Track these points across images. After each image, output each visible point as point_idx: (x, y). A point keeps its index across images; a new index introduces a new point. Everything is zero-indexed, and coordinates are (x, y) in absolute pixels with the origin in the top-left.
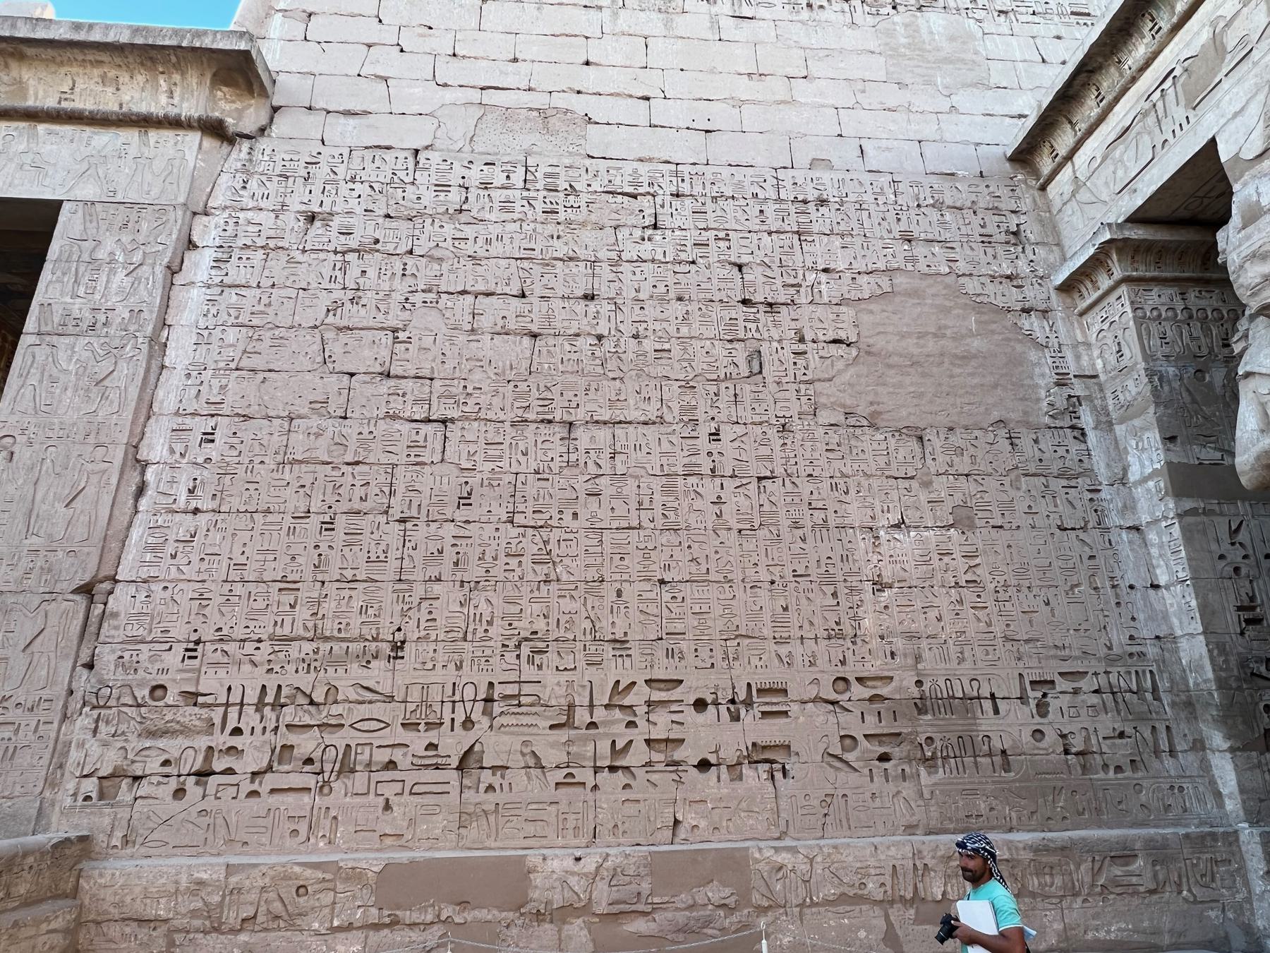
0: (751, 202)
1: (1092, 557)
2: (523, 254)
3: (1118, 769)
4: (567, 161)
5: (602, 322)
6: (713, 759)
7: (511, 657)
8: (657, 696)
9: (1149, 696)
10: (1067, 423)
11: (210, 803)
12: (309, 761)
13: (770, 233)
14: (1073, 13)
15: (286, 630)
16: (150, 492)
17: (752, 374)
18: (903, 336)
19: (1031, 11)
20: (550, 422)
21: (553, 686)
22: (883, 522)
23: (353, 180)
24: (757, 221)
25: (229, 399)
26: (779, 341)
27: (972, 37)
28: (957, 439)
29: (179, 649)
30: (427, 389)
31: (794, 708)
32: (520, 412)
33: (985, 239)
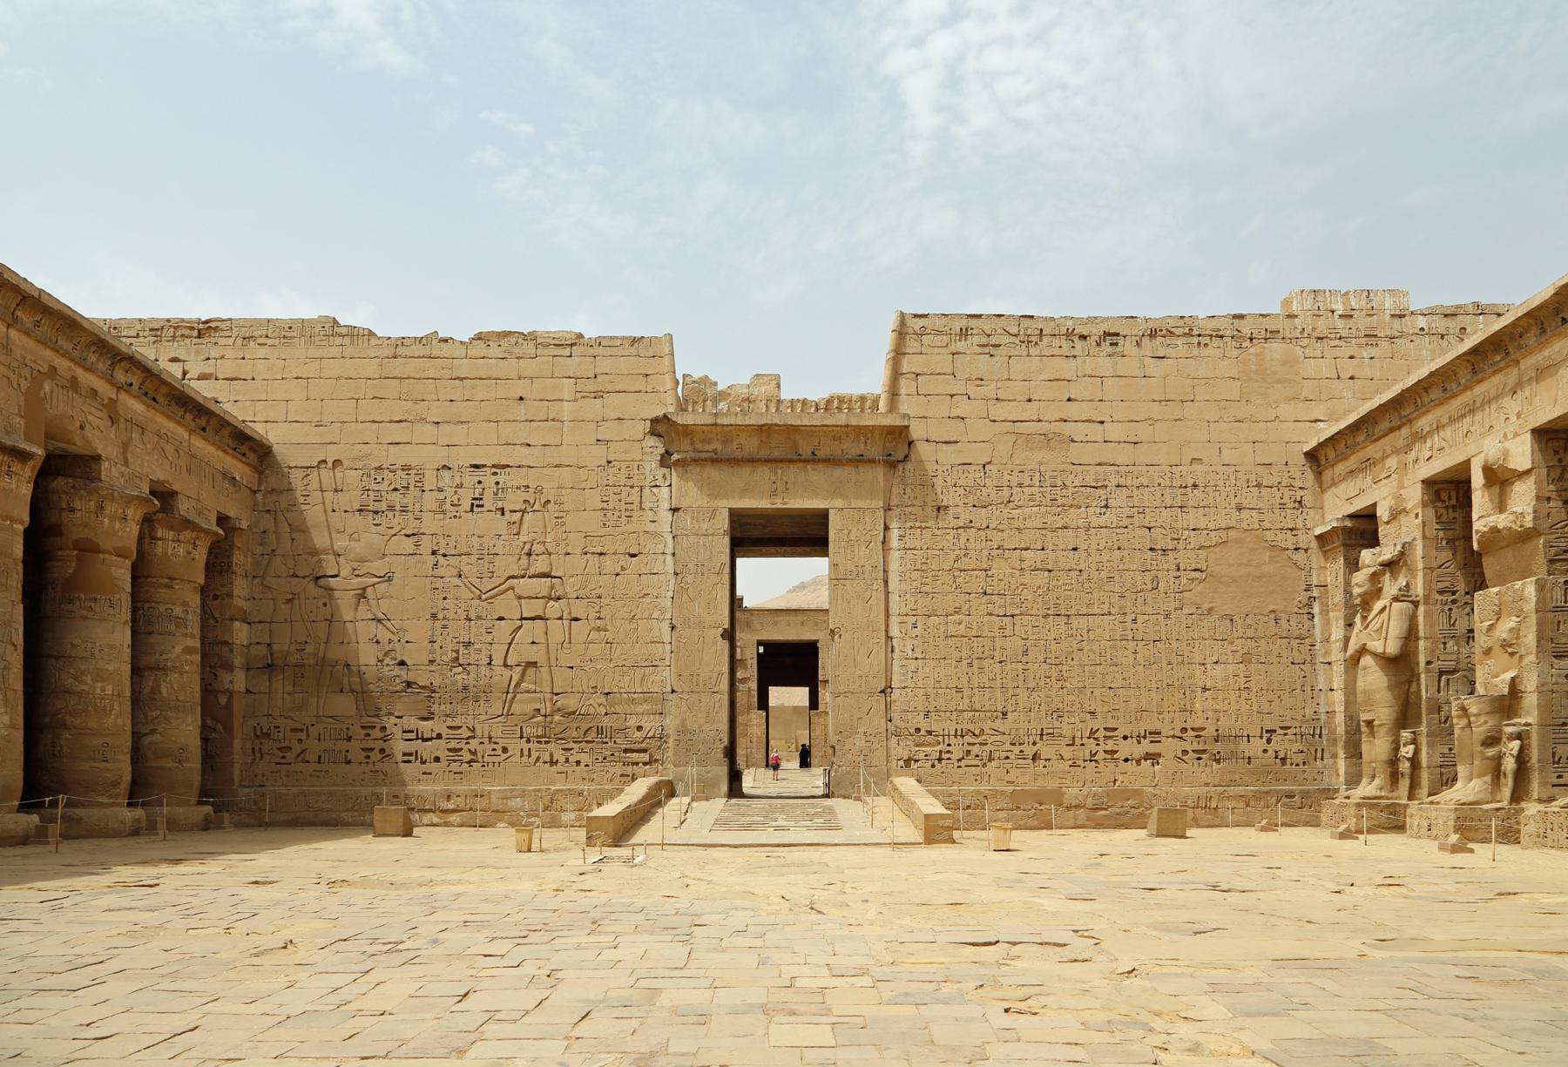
0: (1157, 488)
1: (1305, 677)
2: (1041, 526)
3: (1297, 765)
4: (1061, 467)
5: (1082, 561)
6: (1130, 758)
7: (1049, 718)
8: (1108, 734)
9: (1317, 737)
10: (1306, 611)
11: (944, 770)
12: (977, 756)
13: (1166, 508)
14: (1366, 336)
15: (961, 707)
16: (897, 651)
17: (1153, 589)
18: (1230, 565)
19: (1338, 336)
20: (1059, 615)
21: (1067, 730)
22: (1208, 661)
23: (955, 486)
24: (1159, 501)
25: (919, 606)
26: (1168, 571)
27: (1296, 361)
28: (1248, 621)
29: (922, 714)
30: (1003, 600)
31: (1163, 739)
32: (1046, 611)
33: (1281, 506)
